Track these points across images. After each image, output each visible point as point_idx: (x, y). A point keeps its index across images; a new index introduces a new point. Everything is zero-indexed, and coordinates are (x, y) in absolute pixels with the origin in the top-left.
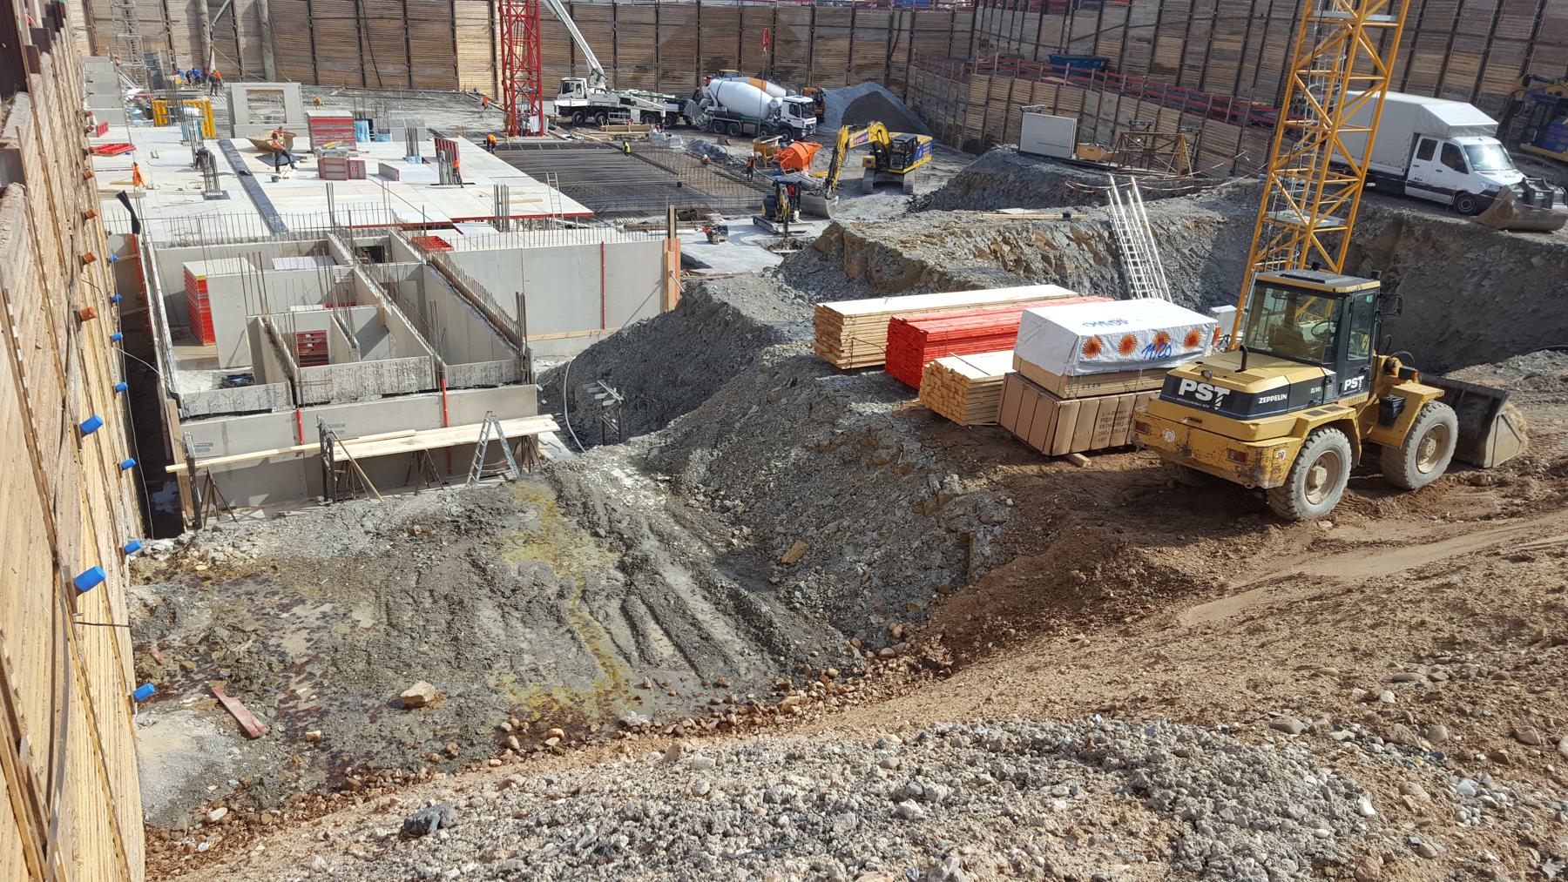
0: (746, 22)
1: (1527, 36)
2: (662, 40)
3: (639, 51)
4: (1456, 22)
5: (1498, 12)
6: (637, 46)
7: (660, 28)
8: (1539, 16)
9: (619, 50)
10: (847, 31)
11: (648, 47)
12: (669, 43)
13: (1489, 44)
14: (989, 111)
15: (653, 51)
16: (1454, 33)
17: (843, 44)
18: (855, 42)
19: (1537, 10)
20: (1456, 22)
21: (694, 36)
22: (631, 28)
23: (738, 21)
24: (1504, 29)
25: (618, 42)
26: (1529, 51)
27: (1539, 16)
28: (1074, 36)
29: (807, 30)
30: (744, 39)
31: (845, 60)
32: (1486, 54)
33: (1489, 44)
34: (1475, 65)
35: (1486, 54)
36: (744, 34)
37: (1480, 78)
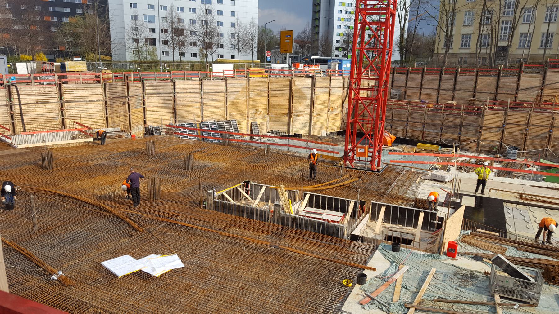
0: (271, 87)
2: (229, 102)
3: (216, 110)
6: (215, 107)
7: (228, 94)
9: (204, 111)
10: (328, 90)
11: (221, 107)
12: (233, 103)
14: (506, 130)
15: (223, 109)
17: (326, 97)
18: (331, 95)
21: (246, 98)
22: (212, 95)
23: (267, 87)
25: (204, 106)
28: (520, 87)
29: (310, 90)
30: (271, 97)
31: (327, 105)
36: (270, 95)
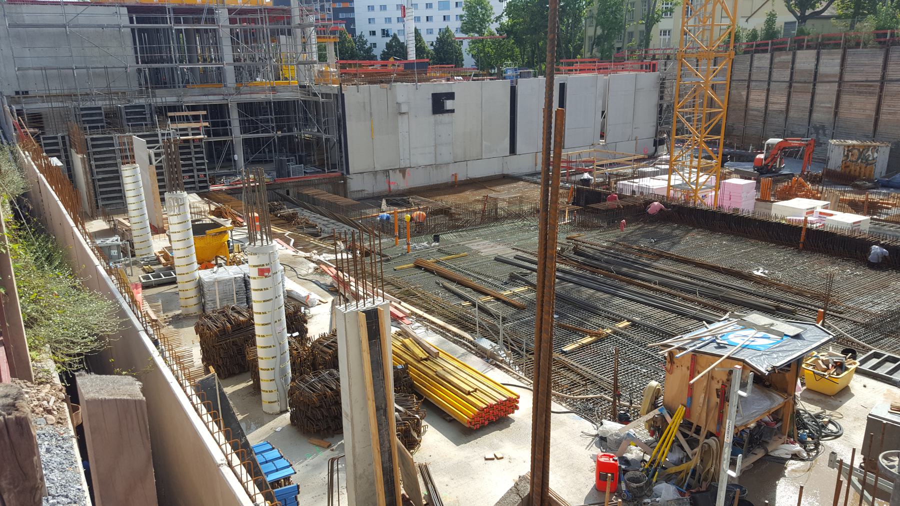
1: (788, 79)
4: (750, 75)
5: (771, 68)
8: (792, 68)
13: (769, 85)
16: (749, 80)
19: (790, 65)
20: (750, 75)
24: (776, 75)
26: (790, 87)
27: (792, 68)
32: (768, 90)
33: (769, 85)
34: (763, 96)
35: (768, 90)
37: (767, 103)
